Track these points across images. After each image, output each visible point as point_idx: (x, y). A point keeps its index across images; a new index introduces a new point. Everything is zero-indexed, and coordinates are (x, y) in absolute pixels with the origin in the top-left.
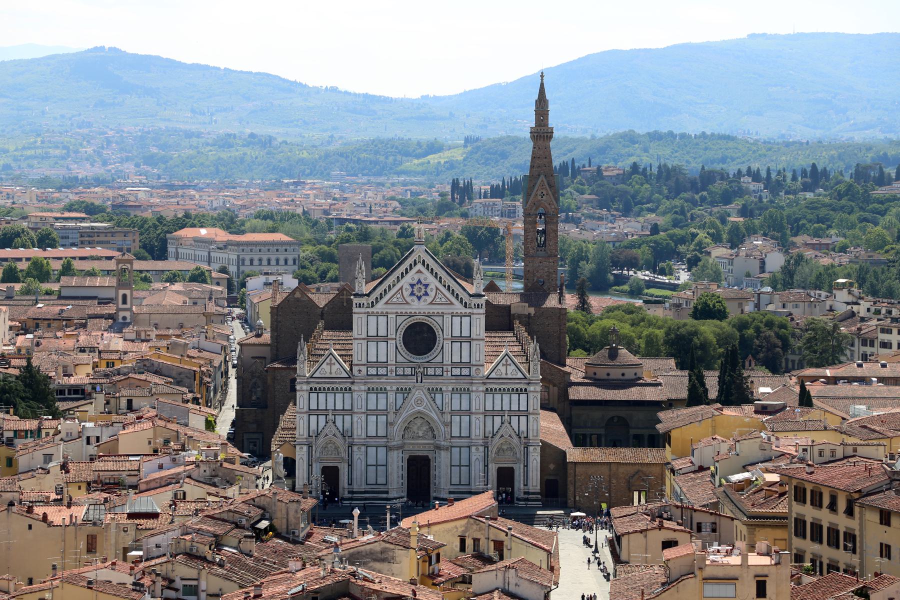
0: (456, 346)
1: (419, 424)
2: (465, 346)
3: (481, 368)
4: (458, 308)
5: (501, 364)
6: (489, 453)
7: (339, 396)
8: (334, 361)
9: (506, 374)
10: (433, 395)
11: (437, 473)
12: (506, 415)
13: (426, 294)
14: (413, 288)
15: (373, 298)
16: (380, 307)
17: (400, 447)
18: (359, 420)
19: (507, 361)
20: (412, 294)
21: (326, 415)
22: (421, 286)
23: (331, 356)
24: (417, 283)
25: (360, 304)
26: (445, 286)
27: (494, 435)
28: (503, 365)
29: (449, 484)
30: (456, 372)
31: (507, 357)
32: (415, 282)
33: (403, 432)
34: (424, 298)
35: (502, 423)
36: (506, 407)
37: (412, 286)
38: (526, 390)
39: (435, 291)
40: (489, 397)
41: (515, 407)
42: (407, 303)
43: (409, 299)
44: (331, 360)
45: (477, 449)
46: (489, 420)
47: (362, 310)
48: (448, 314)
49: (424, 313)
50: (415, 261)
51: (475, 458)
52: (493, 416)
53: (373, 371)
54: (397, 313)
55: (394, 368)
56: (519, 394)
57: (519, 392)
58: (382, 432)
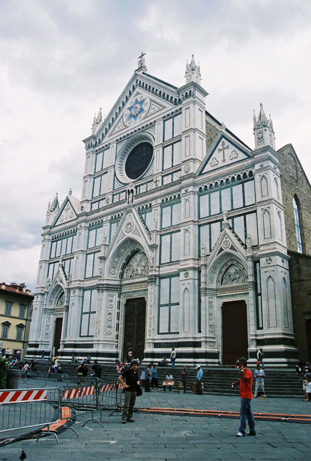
1: (138, 260)
3: (191, 164)
4: (169, 107)
5: (217, 150)
9: (224, 161)
10: (143, 216)
13: (142, 110)
17: (118, 288)
23: (68, 202)
28: (219, 150)
30: (168, 180)
31: (223, 139)
33: (120, 271)
37: (130, 109)
38: (251, 173)
39: (149, 105)
40: (204, 199)
43: (127, 124)
44: (68, 206)
46: (205, 230)
47: (92, 149)
49: (139, 129)
53: (95, 206)
56: (243, 183)
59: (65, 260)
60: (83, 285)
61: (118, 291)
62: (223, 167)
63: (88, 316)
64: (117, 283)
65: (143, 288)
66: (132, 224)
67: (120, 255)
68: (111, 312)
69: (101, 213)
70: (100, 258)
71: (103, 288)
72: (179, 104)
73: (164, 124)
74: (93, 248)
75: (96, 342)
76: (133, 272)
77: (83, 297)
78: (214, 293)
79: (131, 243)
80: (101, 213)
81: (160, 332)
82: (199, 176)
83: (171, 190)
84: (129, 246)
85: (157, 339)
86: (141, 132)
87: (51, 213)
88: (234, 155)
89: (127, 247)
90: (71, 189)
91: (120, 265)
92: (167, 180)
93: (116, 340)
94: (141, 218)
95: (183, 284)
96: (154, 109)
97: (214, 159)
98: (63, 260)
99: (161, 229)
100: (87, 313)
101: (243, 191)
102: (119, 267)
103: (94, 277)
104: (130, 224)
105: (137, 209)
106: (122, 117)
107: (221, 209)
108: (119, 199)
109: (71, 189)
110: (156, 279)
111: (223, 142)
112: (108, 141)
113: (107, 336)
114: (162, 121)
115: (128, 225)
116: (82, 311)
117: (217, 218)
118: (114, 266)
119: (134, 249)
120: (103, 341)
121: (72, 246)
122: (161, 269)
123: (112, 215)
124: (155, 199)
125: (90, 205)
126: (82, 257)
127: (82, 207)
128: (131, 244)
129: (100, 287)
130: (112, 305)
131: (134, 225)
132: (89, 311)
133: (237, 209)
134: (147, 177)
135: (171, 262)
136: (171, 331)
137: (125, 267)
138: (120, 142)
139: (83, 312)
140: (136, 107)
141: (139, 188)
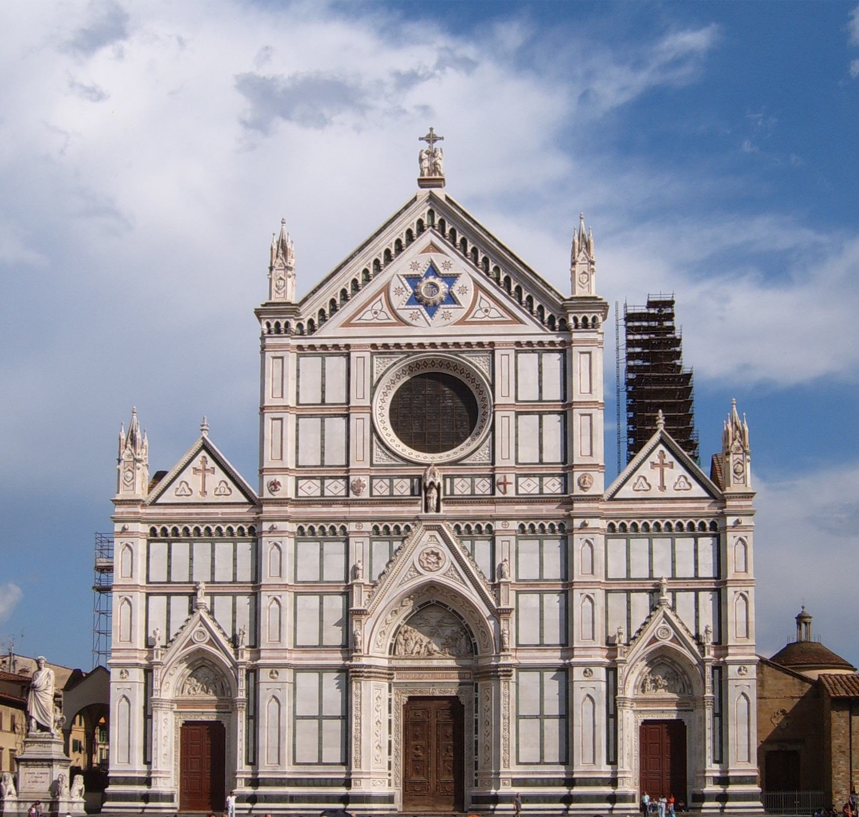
0: (529, 423)
2: (553, 423)
4: (531, 330)
5: (647, 463)
7: (224, 549)
8: (211, 463)
10: (467, 544)
12: (665, 590)
13: (451, 299)
14: (414, 287)
15: (309, 312)
16: (331, 331)
18: (275, 605)
22: (437, 281)
24: (427, 276)
25: (278, 324)
27: (631, 639)
29: (513, 761)
31: (661, 447)
32: (421, 271)
35: (653, 608)
36: (662, 572)
37: (414, 280)
40: (618, 545)
41: (685, 569)
42: (402, 322)
43: (405, 315)
48: (506, 344)
49: (444, 345)
50: (420, 222)
52: (628, 592)
53: (310, 489)
54: (374, 346)
56: (696, 537)
57: (693, 531)
58: (335, 636)
60: (296, 659)
62: (660, 499)
63: (317, 725)
66: (440, 555)
69: (338, 510)
71: (366, 672)
73: (516, 357)
74: (315, 582)
77: (295, 684)
80: (338, 510)
83: (542, 510)
85: (518, 773)
86: (450, 352)
87: (138, 465)
88: (683, 484)
92: (529, 485)
94: (464, 548)
96: (486, 311)
97: (642, 479)
99: (517, 580)
101: (696, 551)
103: (327, 646)
105: (452, 526)
106: (386, 289)
107: (651, 571)
108: (391, 490)
110: (510, 671)
121: (235, 566)
122: (518, 654)
126: (287, 599)
131: (447, 558)
132: (317, 714)
133: (685, 579)
134: (473, 464)
135: (540, 645)
140: (434, 285)
141: (452, 483)
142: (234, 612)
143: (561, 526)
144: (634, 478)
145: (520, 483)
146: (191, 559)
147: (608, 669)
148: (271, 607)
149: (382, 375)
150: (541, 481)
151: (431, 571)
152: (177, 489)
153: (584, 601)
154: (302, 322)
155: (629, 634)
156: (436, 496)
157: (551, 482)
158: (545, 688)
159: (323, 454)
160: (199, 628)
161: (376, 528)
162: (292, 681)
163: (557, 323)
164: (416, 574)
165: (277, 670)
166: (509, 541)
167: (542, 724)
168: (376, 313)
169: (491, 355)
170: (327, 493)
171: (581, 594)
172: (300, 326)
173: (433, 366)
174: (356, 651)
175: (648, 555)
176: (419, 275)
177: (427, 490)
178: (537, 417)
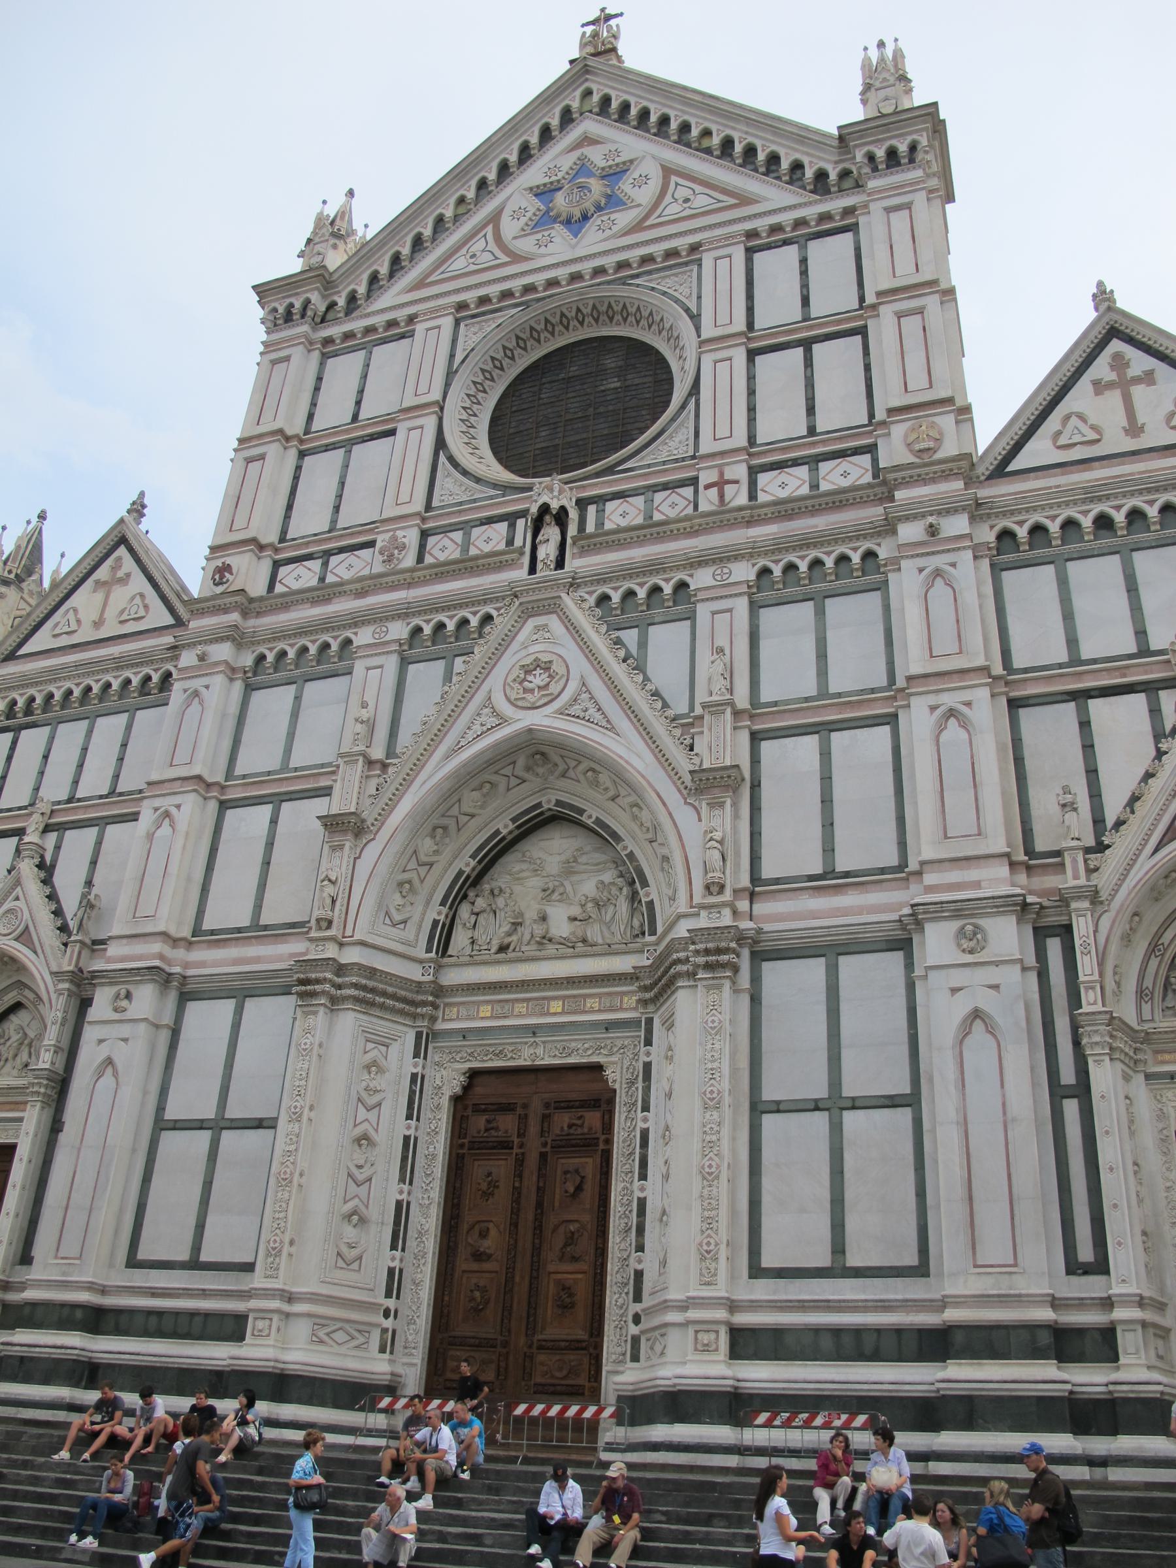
1: (553, 864)
3: (946, 422)
6: (1086, 967)
7: (110, 727)
8: (129, 564)
9: (1134, 429)
10: (630, 637)
11: (652, 1190)
13: (612, 201)
19: (1119, 362)
20: (545, 220)
21: (20, 832)
23: (122, 551)
26: (708, 151)
28: (1099, 387)
33: (437, 912)
34: (596, 221)
39: (654, 186)
43: (526, 245)
45: (972, 940)
49: (599, 271)
51: (961, 1007)
52: (1081, 696)
54: (462, 306)
55: (411, 537)
59: (62, 827)
60: (186, 965)
61: (414, 1016)
62: (1134, 453)
64: (414, 973)
65: (592, 1011)
66: (558, 667)
67: (451, 823)
68: (372, 1132)
70: (333, 824)
71: (339, 987)
72: (840, 191)
74: (269, 773)
75: (275, 1304)
76: (516, 925)
77: (175, 1033)
78: (1131, 1054)
79: (528, 769)
81: (765, 1263)
82: (989, 478)
84: (514, 781)
85: (754, 1306)
86: (609, 283)
89: (502, 787)
90: (142, 494)
91: (442, 881)
92: (783, 485)
93: (391, 1303)
94: (618, 642)
95: (954, 991)
96: (687, 200)
98: (47, 829)
100: (199, 1125)
102: (434, 889)
103: (266, 928)
104: (547, 669)
105: (592, 600)
106: (495, 219)
107: (1141, 633)
109: (142, 494)
111: (1117, 356)
112: (403, 305)
113: (340, 1275)
114: (741, 248)
115: (528, 672)
116: (161, 1108)
117: (1124, 676)
118: (410, 882)
119: (539, 805)
120: (314, 1298)
122: (760, 908)
123: (416, 621)
124: (714, 561)
125: (264, 568)
127: (225, 569)
128: (526, 776)
129: (318, 981)
130: (376, 1091)
132: (210, 1113)
134: (649, 466)
135: (829, 873)
136: (854, 1260)
137: (465, 896)
138: (474, 316)
139: (170, 1114)
141: (600, 512)
142: (94, 863)
143: (870, 555)
144: (1053, 422)
145: (760, 486)
146: (46, 757)
147: (1041, 934)
148: (159, 833)
149: (473, 350)
150: (814, 470)
151: (534, 708)
152: (57, 625)
153: (941, 728)
154: (336, 298)
155: (1098, 821)
156: (559, 538)
157: (840, 470)
158: (844, 1007)
159: (337, 509)
160: (17, 903)
161: (418, 630)
162: (168, 1019)
163: (833, 176)
164: (494, 721)
165: (131, 987)
166: (730, 610)
167: (836, 1129)
168: (473, 256)
169: (695, 268)
170: (330, 578)
171: (933, 708)
172: (332, 306)
173: (582, 323)
174: (320, 928)
175: (1124, 595)
176: (558, 181)
177: (537, 526)
178: (800, 351)
